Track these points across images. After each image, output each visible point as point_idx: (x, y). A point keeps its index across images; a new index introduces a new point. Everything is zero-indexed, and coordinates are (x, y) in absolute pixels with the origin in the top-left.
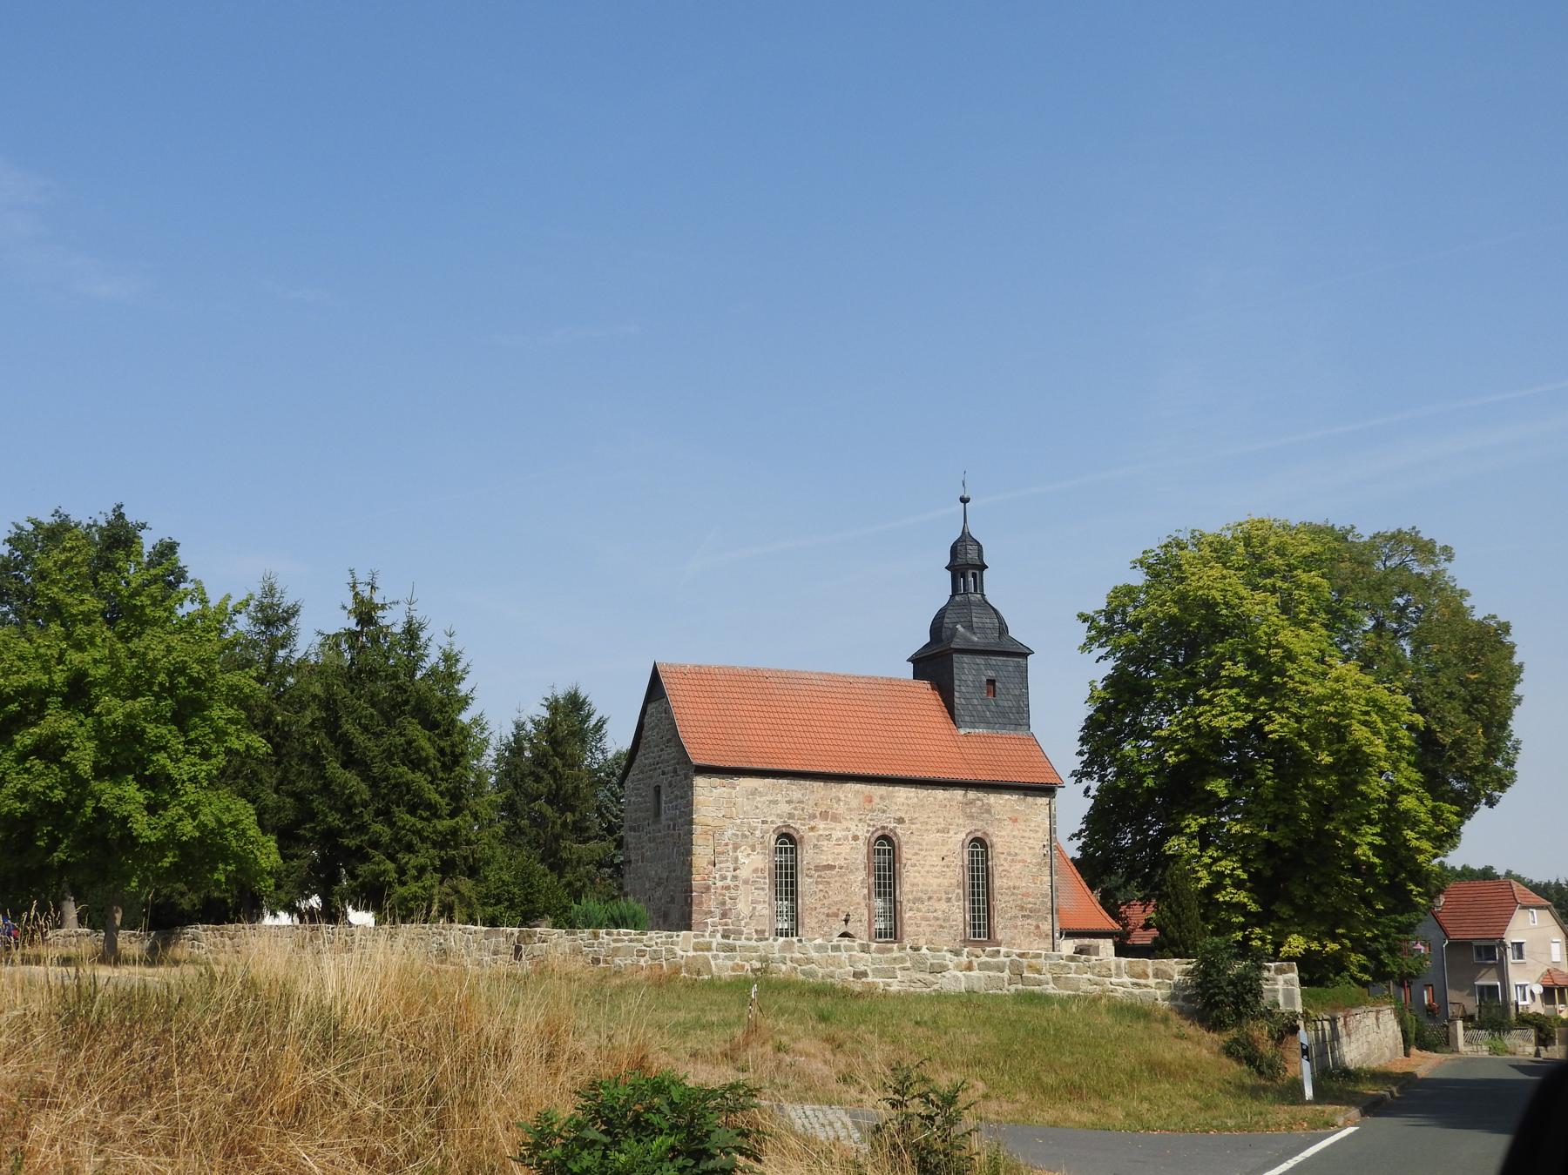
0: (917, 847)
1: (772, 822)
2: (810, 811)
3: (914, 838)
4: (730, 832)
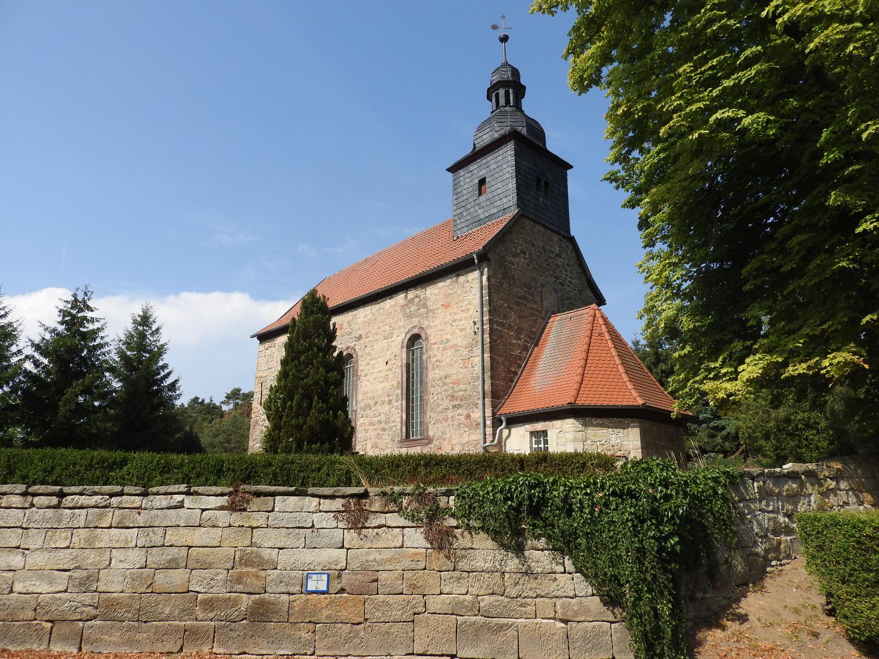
0: (369, 357)
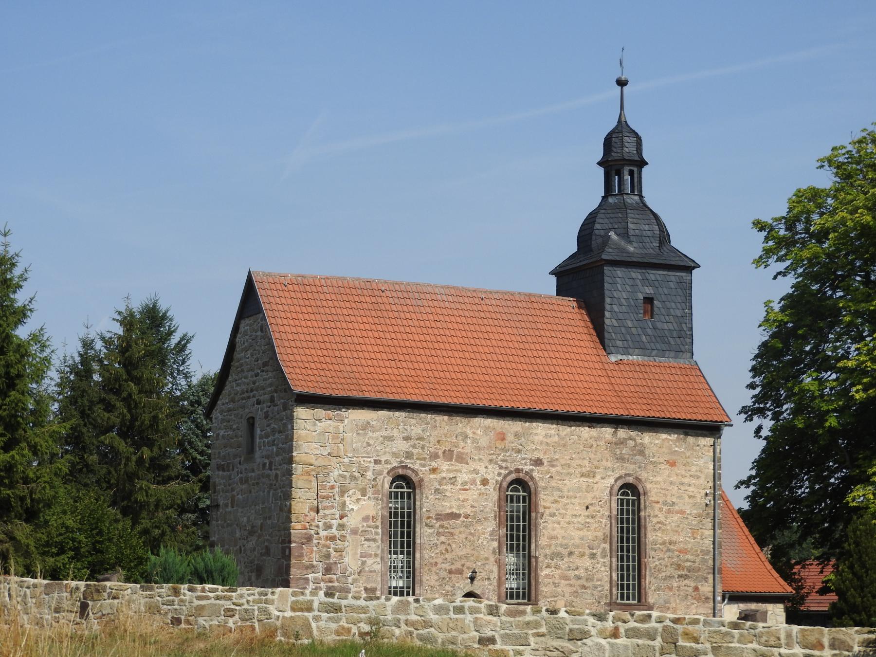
0: (556, 493)
1: (387, 462)
2: (432, 450)
3: (553, 483)
4: (336, 473)
